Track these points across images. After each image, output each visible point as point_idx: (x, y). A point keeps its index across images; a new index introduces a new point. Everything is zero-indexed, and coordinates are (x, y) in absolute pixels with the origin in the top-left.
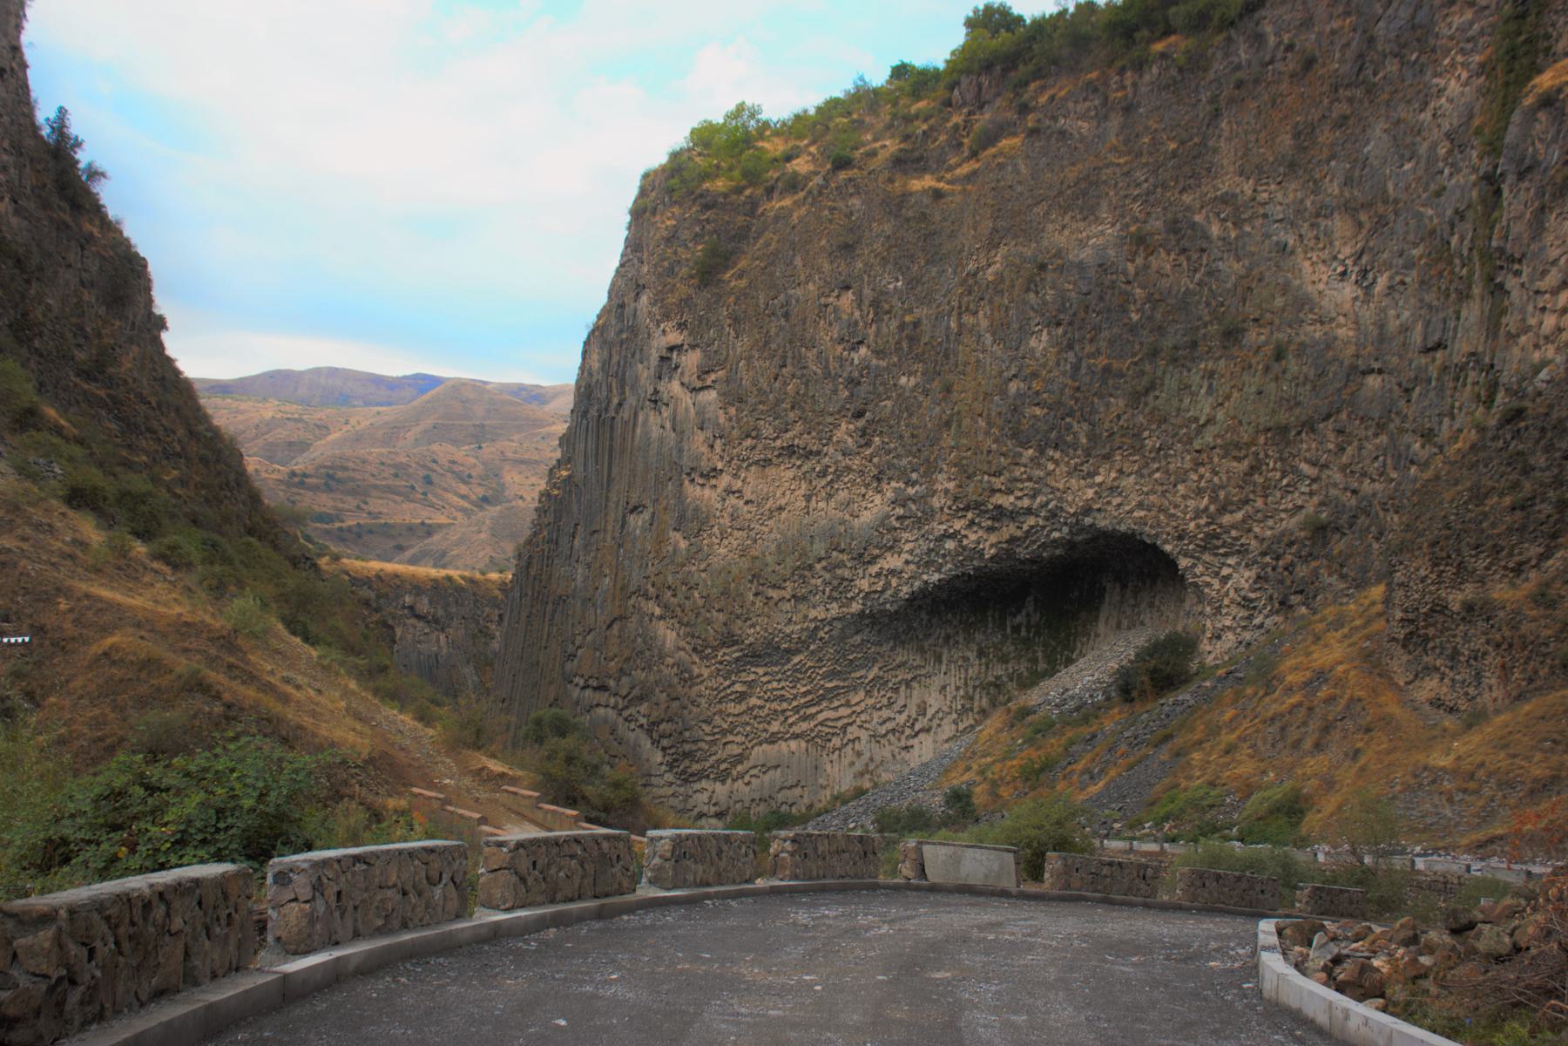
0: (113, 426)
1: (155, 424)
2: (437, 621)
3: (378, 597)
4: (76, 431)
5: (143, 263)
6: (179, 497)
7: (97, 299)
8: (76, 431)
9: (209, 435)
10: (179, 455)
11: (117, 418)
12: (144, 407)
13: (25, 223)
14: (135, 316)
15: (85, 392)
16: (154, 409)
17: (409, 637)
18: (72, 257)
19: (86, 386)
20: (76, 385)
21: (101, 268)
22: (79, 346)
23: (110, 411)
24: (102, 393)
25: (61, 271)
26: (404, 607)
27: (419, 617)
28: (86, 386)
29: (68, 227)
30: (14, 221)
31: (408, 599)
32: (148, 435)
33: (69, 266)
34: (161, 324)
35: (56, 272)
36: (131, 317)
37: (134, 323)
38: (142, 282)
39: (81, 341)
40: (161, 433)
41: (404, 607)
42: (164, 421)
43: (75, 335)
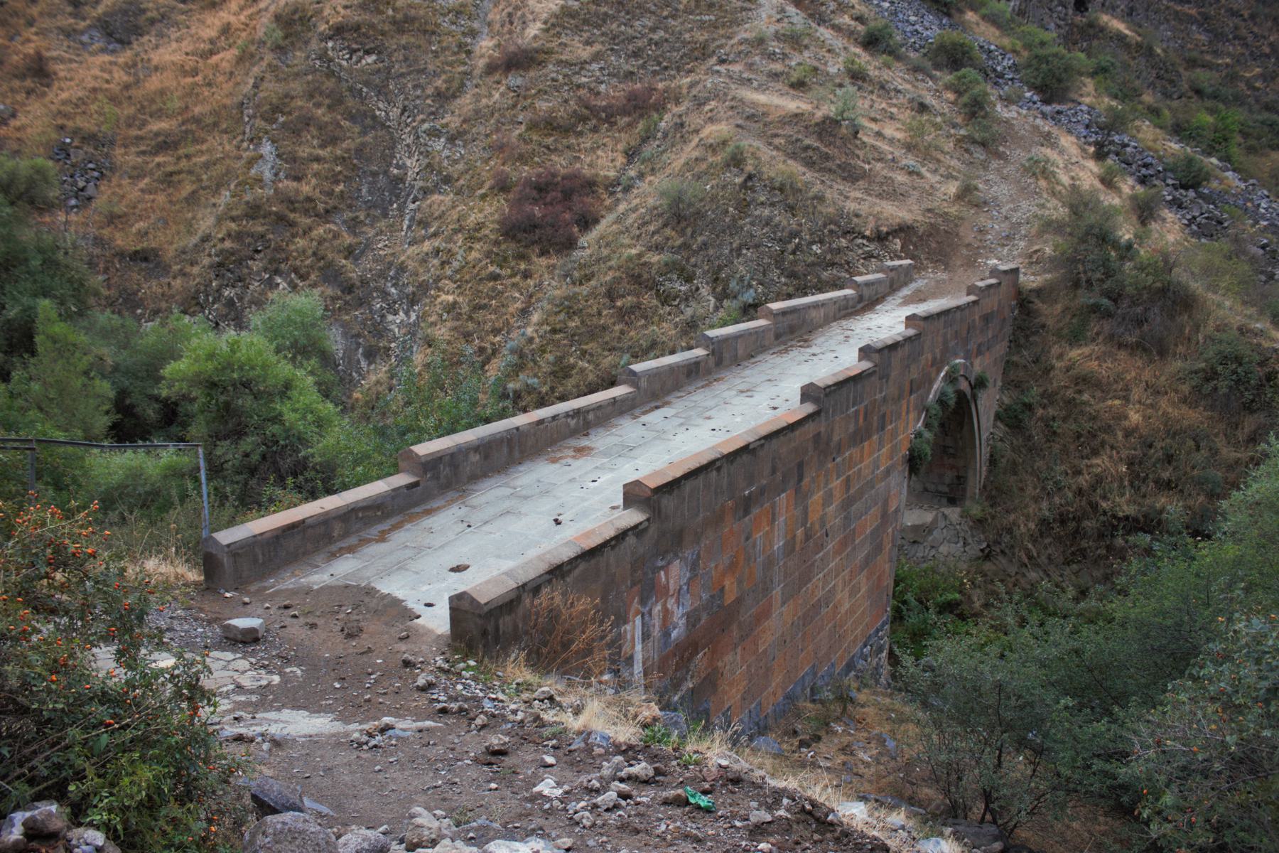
0: (1203, 37)
1: (1244, 32)
4: (1139, 39)
6: (1258, 89)
8: (1139, 39)
10: (1268, 56)
11: (1206, 30)
12: (1237, 20)
15: (1177, 12)
16: (1245, 20)
19: (1179, 8)
20: (1168, 8)
23: (1200, 25)
24: (1193, 12)
28: (1179, 8)
32: (1237, 42)
40: (1250, 39)
42: (1256, 29)
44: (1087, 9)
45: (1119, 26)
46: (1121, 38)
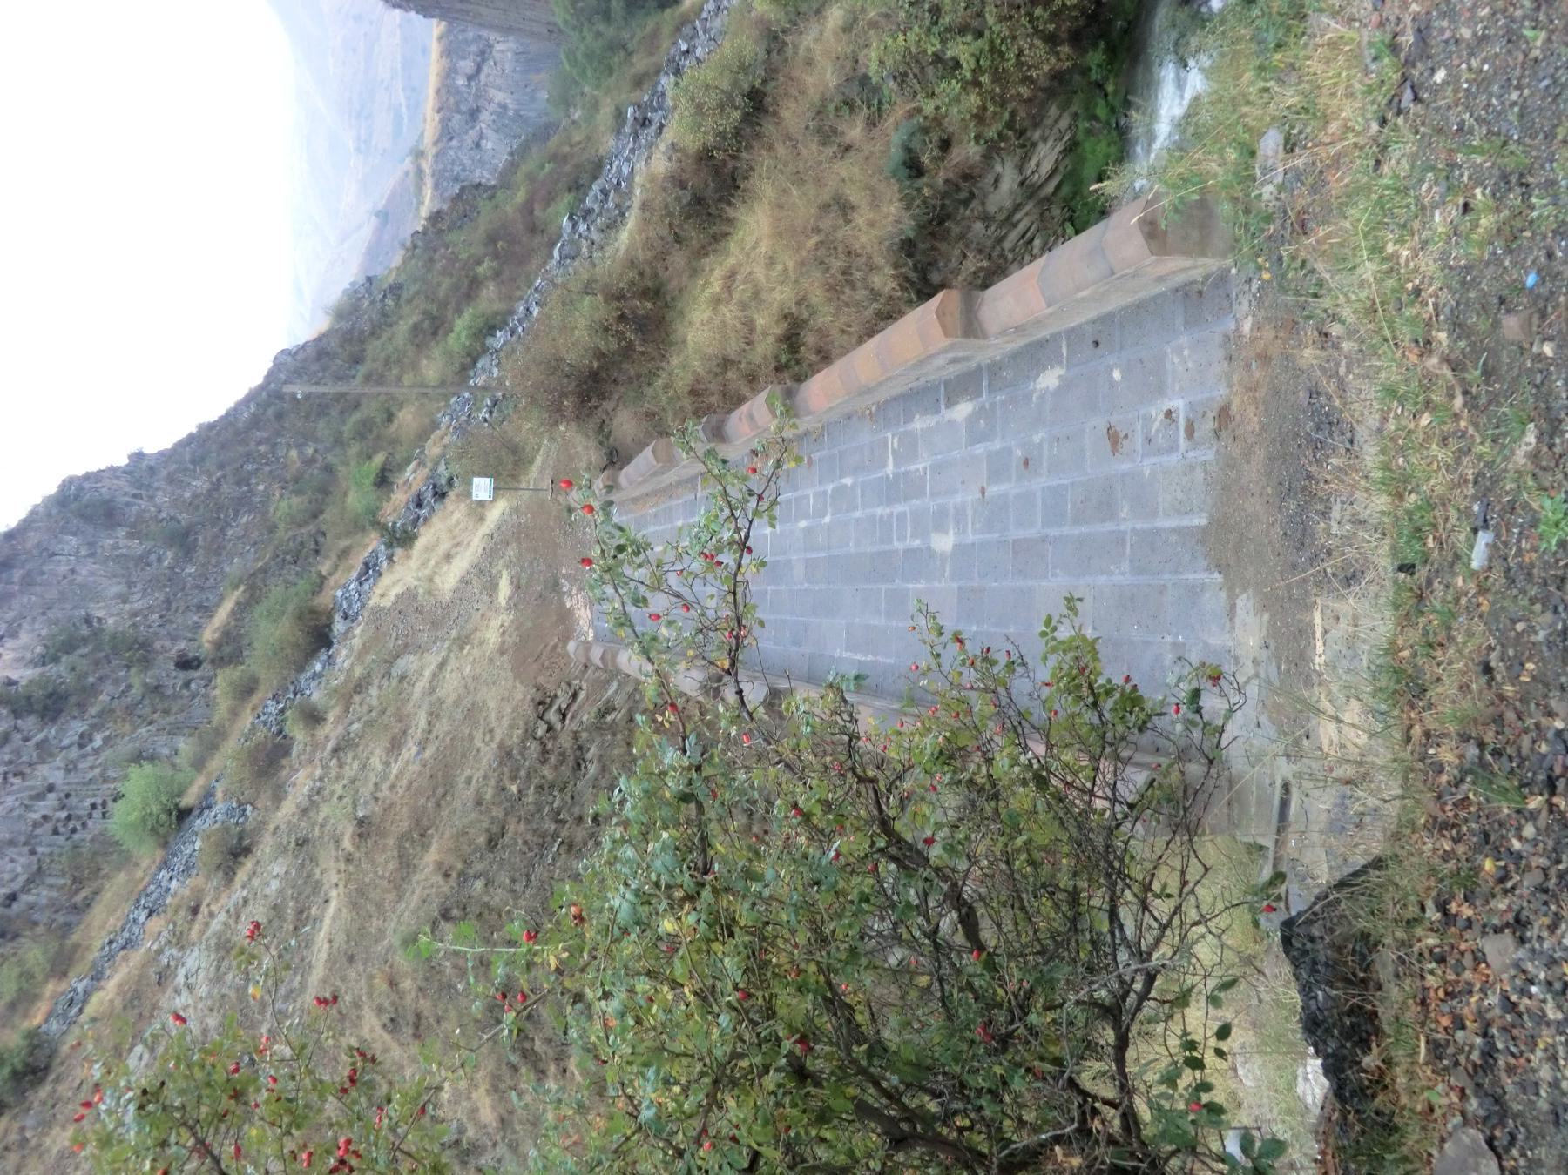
2: (482, 53)
3: (459, 112)
4: (242, 588)
5: (67, 484)
7: (109, 536)
9: (253, 409)
13: (26, 626)
14: (126, 494)
17: (498, 81)
18: (63, 569)
21: (74, 534)
22: (159, 560)
25: (79, 579)
26: (469, 86)
27: (479, 70)
29: (29, 574)
30: (25, 638)
31: (461, 81)
33: (73, 571)
34: (138, 457)
35: (81, 586)
36: (127, 499)
37: (135, 496)
38: (87, 485)
39: (153, 557)
41: (469, 86)
43: (149, 564)
44: (197, 659)
45: (222, 614)
46: (241, 609)
